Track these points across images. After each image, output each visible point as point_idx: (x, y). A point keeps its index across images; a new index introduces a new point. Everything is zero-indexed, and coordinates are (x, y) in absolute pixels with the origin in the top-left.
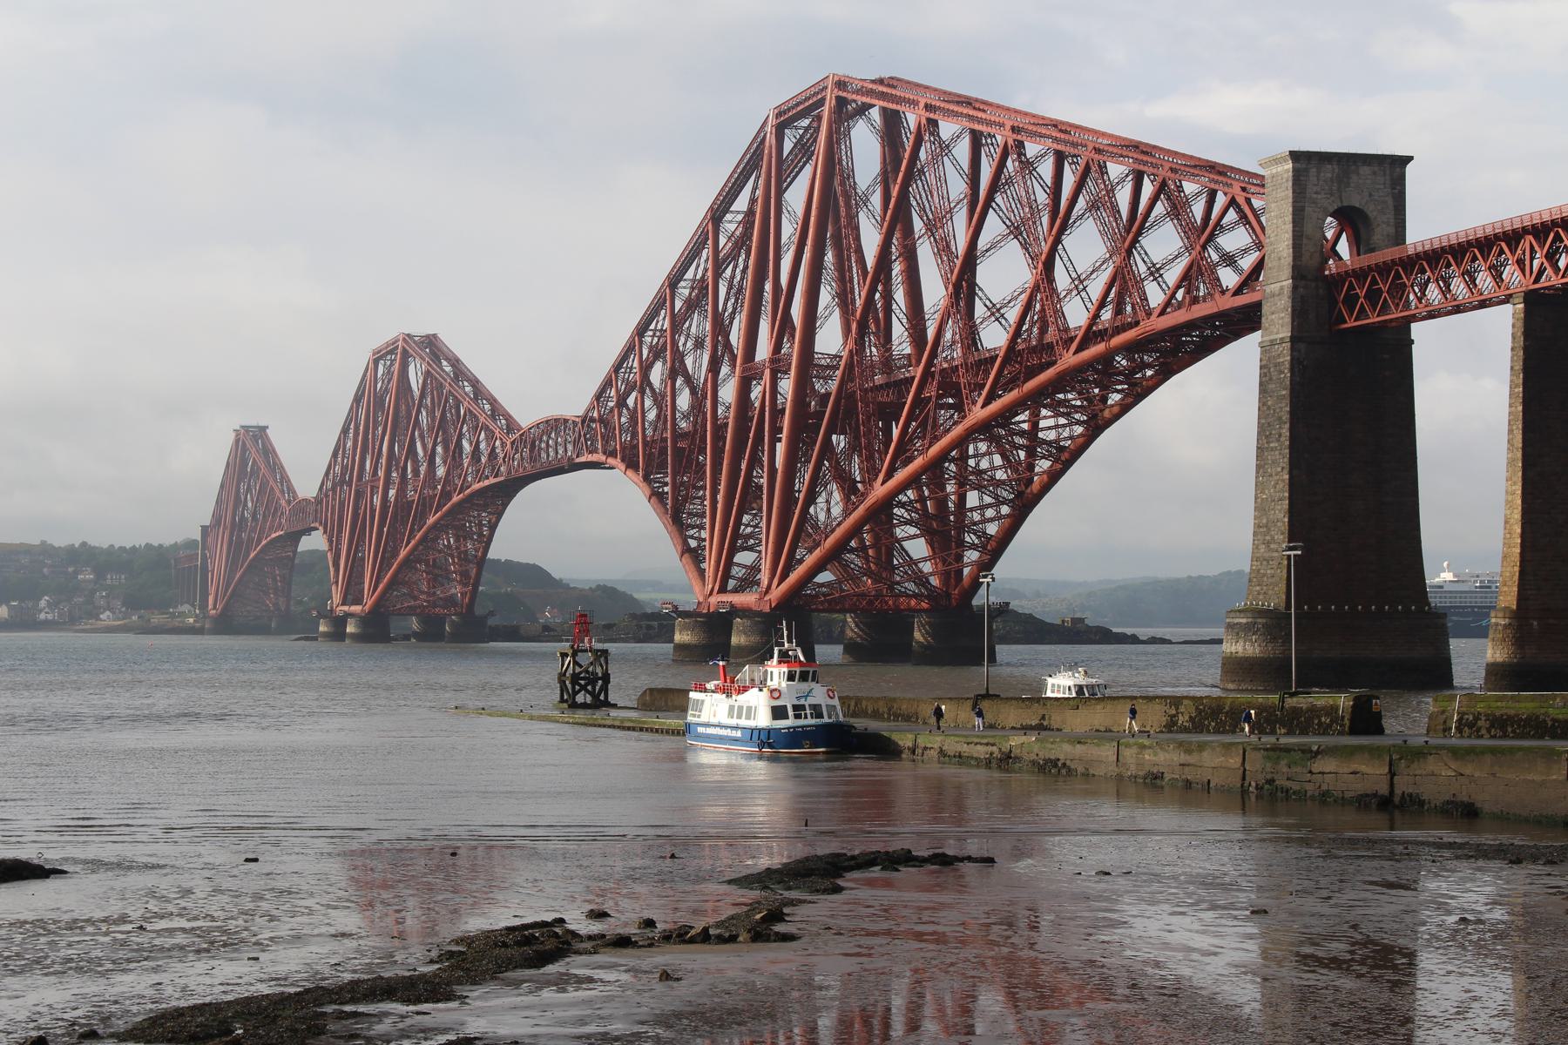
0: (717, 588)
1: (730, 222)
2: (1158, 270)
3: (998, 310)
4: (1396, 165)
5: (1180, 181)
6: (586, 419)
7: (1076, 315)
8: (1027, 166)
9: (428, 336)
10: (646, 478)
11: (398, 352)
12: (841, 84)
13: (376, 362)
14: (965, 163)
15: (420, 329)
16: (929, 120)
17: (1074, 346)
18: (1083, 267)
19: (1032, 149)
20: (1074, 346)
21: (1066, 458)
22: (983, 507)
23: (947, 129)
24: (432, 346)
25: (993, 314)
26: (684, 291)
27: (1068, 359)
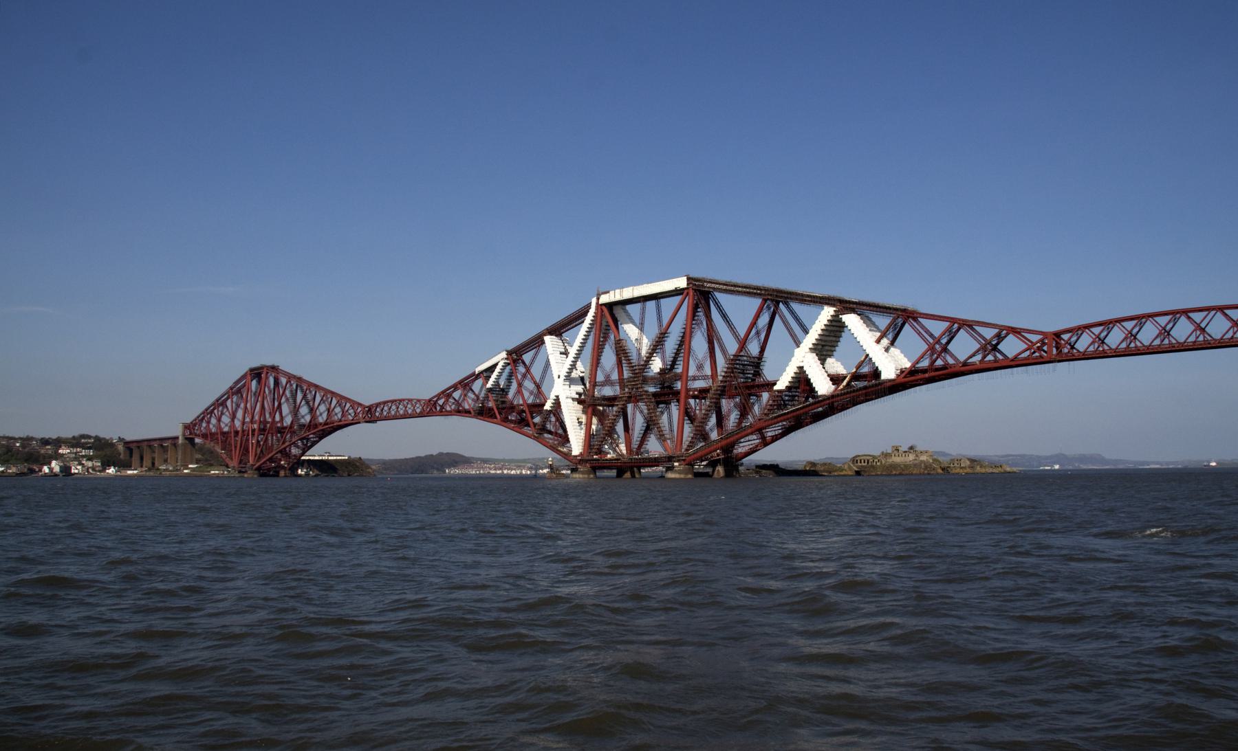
8: (311, 392)
18: (322, 411)
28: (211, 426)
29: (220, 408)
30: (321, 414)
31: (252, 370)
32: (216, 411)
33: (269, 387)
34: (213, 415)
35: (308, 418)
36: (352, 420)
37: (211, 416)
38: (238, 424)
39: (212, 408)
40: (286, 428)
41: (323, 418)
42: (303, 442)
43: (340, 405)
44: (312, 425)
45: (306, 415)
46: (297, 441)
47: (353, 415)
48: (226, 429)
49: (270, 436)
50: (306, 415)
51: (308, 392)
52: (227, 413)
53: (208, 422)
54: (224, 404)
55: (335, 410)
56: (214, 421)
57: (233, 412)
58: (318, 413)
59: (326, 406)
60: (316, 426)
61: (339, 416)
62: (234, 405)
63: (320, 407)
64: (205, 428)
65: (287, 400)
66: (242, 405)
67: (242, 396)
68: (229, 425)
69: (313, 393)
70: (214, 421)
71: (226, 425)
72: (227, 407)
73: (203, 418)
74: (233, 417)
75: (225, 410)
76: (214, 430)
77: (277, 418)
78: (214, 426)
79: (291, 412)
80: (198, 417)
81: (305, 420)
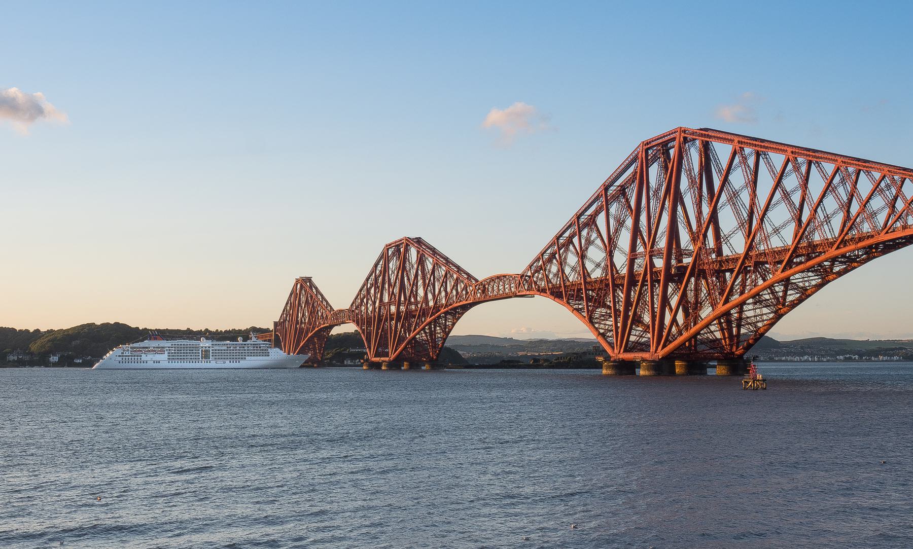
0: (622, 350)
1: (611, 190)
2: (875, 213)
3: (778, 230)
5: (892, 176)
6: (522, 276)
9: (416, 238)
10: (569, 303)
12: (684, 131)
13: (388, 250)
14: (752, 165)
15: (413, 235)
16: (740, 147)
17: (835, 246)
18: (829, 211)
19: (800, 160)
20: (835, 246)
21: (805, 294)
22: (755, 316)
23: (748, 150)
24: (419, 241)
25: (775, 232)
26: (583, 219)
27: (833, 252)
28: (567, 270)
29: (584, 233)
30: (828, 219)
31: (647, 146)
32: (576, 240)
33: (690, 170)
34: (571, 247)
37: (567, 250)
38: (620, 260)
39: (567, 234)
40: (735, 260)
41: (831, 230)
42: (773, 293)
43: (882, 191)
45: (784, 225)
48: (597, 274)
49: (693, 280)
50: (784, 225)
51: (790, 166)
52: (598, 242)
53: (562, 264)
54: (591, 222)
55: (871, 202)
56: (572, 259)
57: (610, 238)
58: (820, 215)
59: (837, 197)
61: (881, 218)
62: (612, 221)
63: (825, 201)
64: (556, 275)
66: (629, 222)
67: (628, 201)
68: (603, 264)
69: (804, 169)
70: (572, 259)
71: (598, 265)
72: (596, 226)
73: (553, 256)
74: (610, 246)
75: (594, 235)
76: (572, 277)
77: (711, 243)
78: (573, 269)
79: (742, 225)
80: (542, 254)
81: (782, 239)
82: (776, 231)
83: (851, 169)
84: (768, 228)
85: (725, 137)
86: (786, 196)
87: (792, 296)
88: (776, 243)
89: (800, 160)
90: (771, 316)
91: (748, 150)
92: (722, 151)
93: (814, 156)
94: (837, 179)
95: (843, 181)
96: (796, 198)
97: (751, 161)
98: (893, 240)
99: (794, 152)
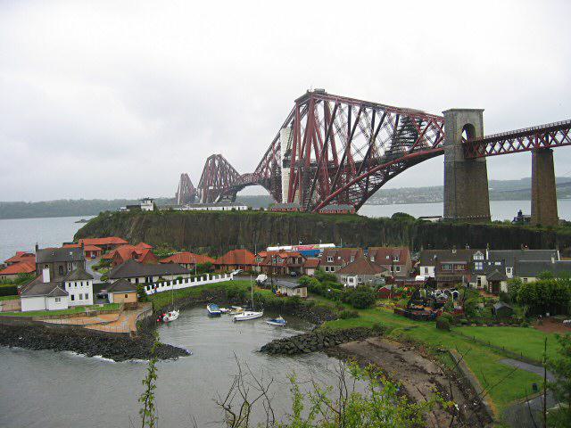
4: (480, 112)
7: (381, 152)
8: (366, 114)
11: (213, 157)
15: (217, 153)
18: (383, 140)
19: (367, 110)
23: (343, 105)
24: (220, 156)
30: (382, 144)
31: (299, 102)
35: (364, 152)
36: (434, 148)
44: (370, 162)
46: (353, 183)
47: (434, 139)
51: (362, 114)
58: (378, 142)
60: (376, 162)
63: (380, 133)
65: (339, 130)
69: (371, 115)
77: (330, 157)
82: (358, 151)
83: (393, 115)
84: (353, 151)
85: (333, 98)
86: (363, 131)
87: (370, 189)
88: (358, 158)
89: (367, 110)
90: (360, 199)
91: (343, 105)
92: (332, 104)
93: (376, 107)
94: (386, 119)
95: (390, 121)
96: (369, 133)
97: (346, 111)
98: (416, 156)
99: (364, 105)
